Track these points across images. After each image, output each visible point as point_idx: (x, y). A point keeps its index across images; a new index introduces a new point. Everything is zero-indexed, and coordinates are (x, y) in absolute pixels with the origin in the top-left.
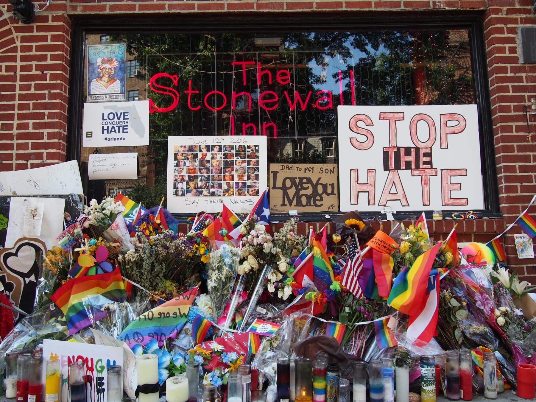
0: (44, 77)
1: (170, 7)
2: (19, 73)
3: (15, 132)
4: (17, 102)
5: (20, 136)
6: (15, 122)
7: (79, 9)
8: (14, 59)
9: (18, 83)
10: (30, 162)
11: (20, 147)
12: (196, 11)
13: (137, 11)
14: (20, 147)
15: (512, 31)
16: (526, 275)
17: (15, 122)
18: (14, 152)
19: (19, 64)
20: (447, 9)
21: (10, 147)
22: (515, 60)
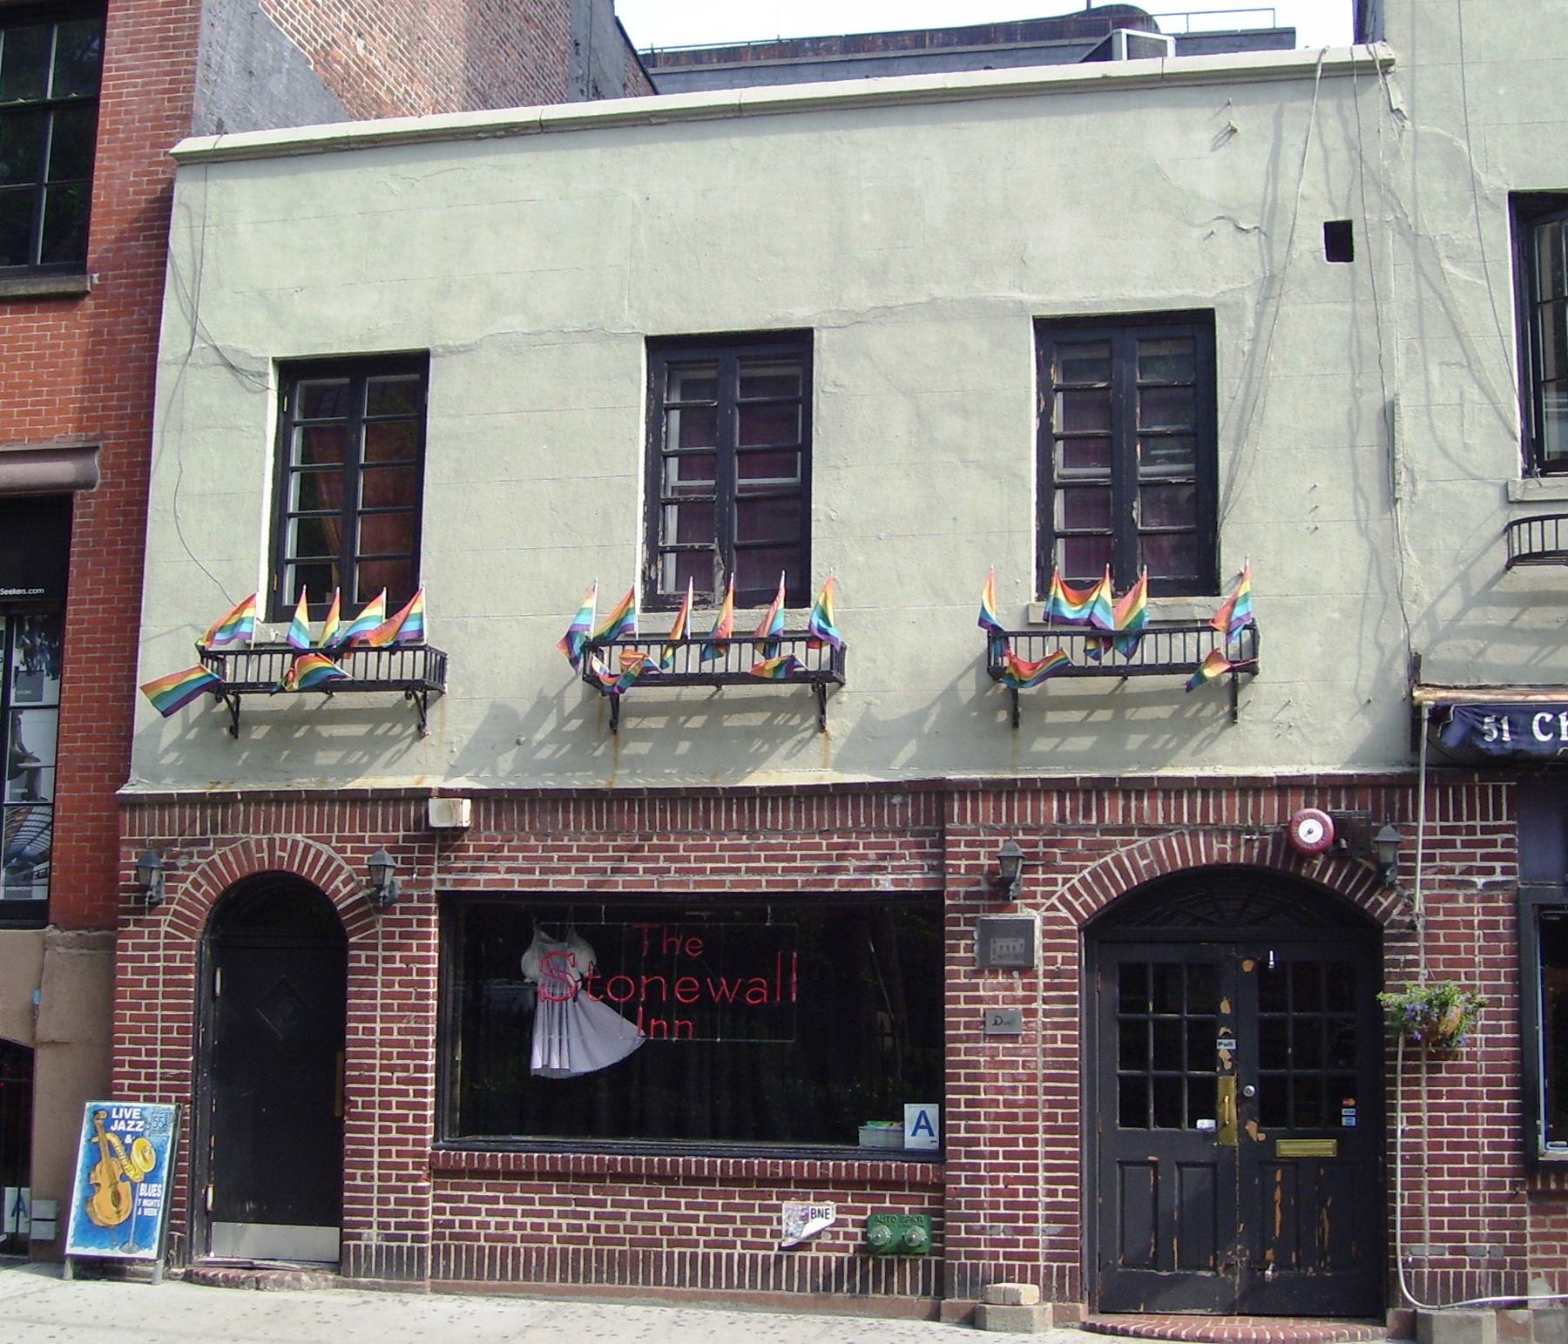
0: (409, 972)
1: (556, 883)
2: (381, 965)
3: (378, 1037)
4: (379, 1001)
5: (383, 1043)
6: (378, 1026)
8: (374, 947)
9: (379, 978)
11: (384, 1056)
13: (516, 888)
14: (384, 1056)
16: (963, 1235)
18: (377, 1062)
19: (380, 953)
20: (892, 889)
21: (372, 1055)
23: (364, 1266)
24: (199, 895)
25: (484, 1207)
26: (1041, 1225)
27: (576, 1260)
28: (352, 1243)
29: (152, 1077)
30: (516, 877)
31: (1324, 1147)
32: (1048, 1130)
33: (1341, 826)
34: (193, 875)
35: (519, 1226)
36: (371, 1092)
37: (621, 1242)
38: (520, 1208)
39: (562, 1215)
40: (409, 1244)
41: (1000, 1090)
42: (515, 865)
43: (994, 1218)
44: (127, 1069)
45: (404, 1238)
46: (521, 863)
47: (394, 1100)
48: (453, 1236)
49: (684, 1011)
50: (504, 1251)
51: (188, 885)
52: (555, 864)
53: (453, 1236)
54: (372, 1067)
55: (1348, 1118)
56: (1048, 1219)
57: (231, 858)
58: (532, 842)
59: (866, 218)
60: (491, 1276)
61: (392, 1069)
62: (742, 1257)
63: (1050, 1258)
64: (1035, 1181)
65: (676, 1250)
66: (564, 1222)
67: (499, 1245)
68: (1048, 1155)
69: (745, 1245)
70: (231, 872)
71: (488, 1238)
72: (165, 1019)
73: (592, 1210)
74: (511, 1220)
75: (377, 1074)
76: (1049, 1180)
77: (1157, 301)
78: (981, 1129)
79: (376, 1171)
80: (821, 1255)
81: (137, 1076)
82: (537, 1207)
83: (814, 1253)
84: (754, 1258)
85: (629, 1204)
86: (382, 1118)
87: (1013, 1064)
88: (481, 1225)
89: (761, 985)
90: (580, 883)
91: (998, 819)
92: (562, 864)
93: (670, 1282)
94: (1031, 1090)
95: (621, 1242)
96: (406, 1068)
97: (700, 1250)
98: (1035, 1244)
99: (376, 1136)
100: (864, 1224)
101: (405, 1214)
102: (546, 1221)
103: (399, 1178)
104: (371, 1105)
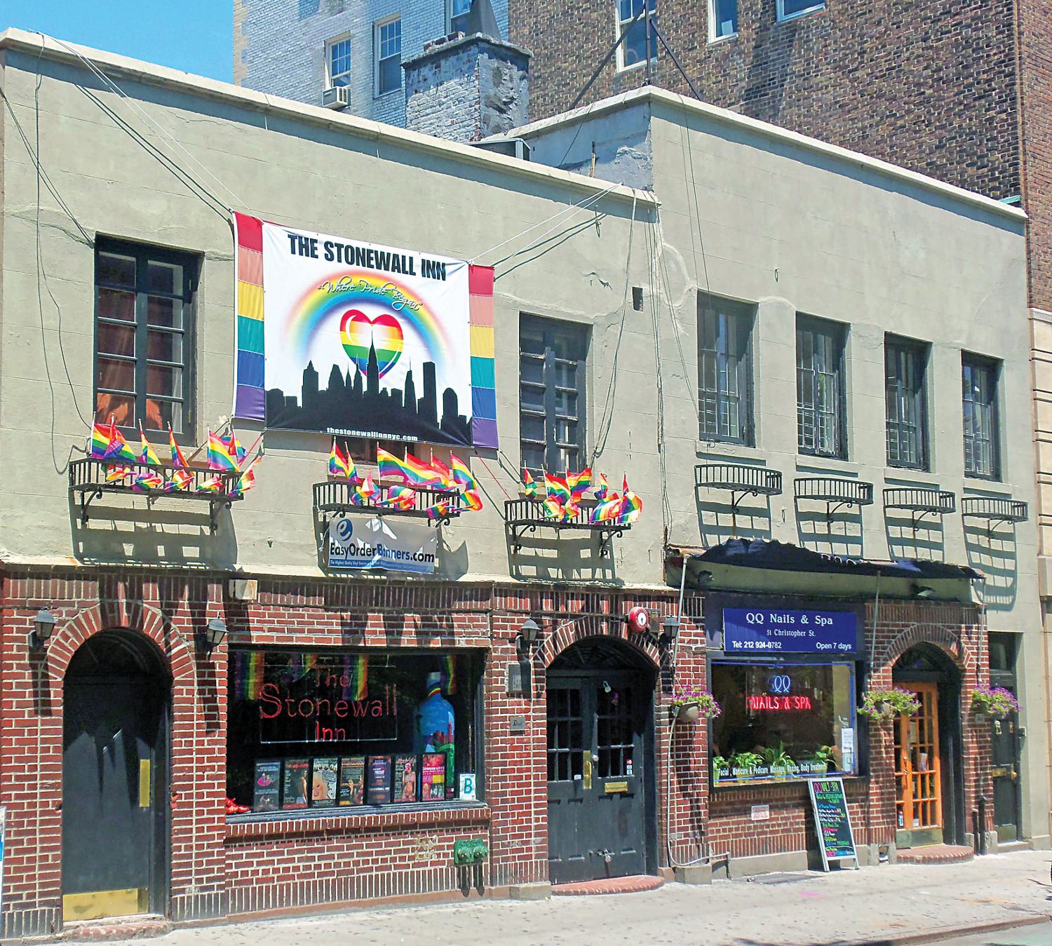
3: (195, 747)
6: (195, 739)
7: (235, 638)
10: (206, 774)
11: (199, 760)
12: (314, 644)
15: (503, 666)
17: (195, 739)
18: (194, 765)
22: (502, 689)
23: (186, 912)
24: (67, 645)
25: (255, 860)
26: (533, 838)
27: (308, 889)
28: (178, 896)
29: (34, 787)
30: (274, 634)
31: (622, 786)
32: (536, 784)
33: (648, 616)
34: (62, 629)
35: (276, 871)
36: (191, 787)
37: (332, 873)
38: (276, 858)
39: (300, 860)
40: (215, 892)
41: (515, 763)
42: (272, 626)
43: (514, 836)
44: (13, 782)
45: (212, 888)
46: (276, 625)
47: (205, 791)
48: (237, 883)
49: (340, 723)
50: (268, 888)
51: (58, 637)
52: (296, 626)
53: (237, 883)
54: (191, 769)
55: (629, 772)
56: (537, 835)
57: (91, 616)
58: (282, 611)
59: (441, 228)
60: (261, 906)
61: (203, 769)
62: (395, 874)
63: (537, 856)
64: (530, 813)
65: (361, 875)
66: (301, 864)
67: (264, 885)
68: (536, 798)
69: (396, 867)
70: (91, 628)
71: (258, 881)
72: (44, 741)
73: (316, 855)
74: (271, 867)
75: (195, 774)
76: (536, 813)
77: (571, 315)
78: (507, 786)
79: (194, 843)
80: (432, 868)
81: (22, 787)
82: (286, 856)
83: (429, 868)
84: (401, 874)
85: (338, 848)
86: (198, 804)
87: (520, 748)
88: (255, 872)
89: (378, 704)
90: (310, 639)
91: (516, 606)
92: (300, 627)
93: (359, 896)
94: (528, 762)
95: (332, 873)
96: (212, 768)
97: (374, 873)
98: (529, 849)
99: (194, 818)
100: (453, 847)
101: (212, 871)
102: (291, 865)
103: (209, 846)
104: (191, 796)
